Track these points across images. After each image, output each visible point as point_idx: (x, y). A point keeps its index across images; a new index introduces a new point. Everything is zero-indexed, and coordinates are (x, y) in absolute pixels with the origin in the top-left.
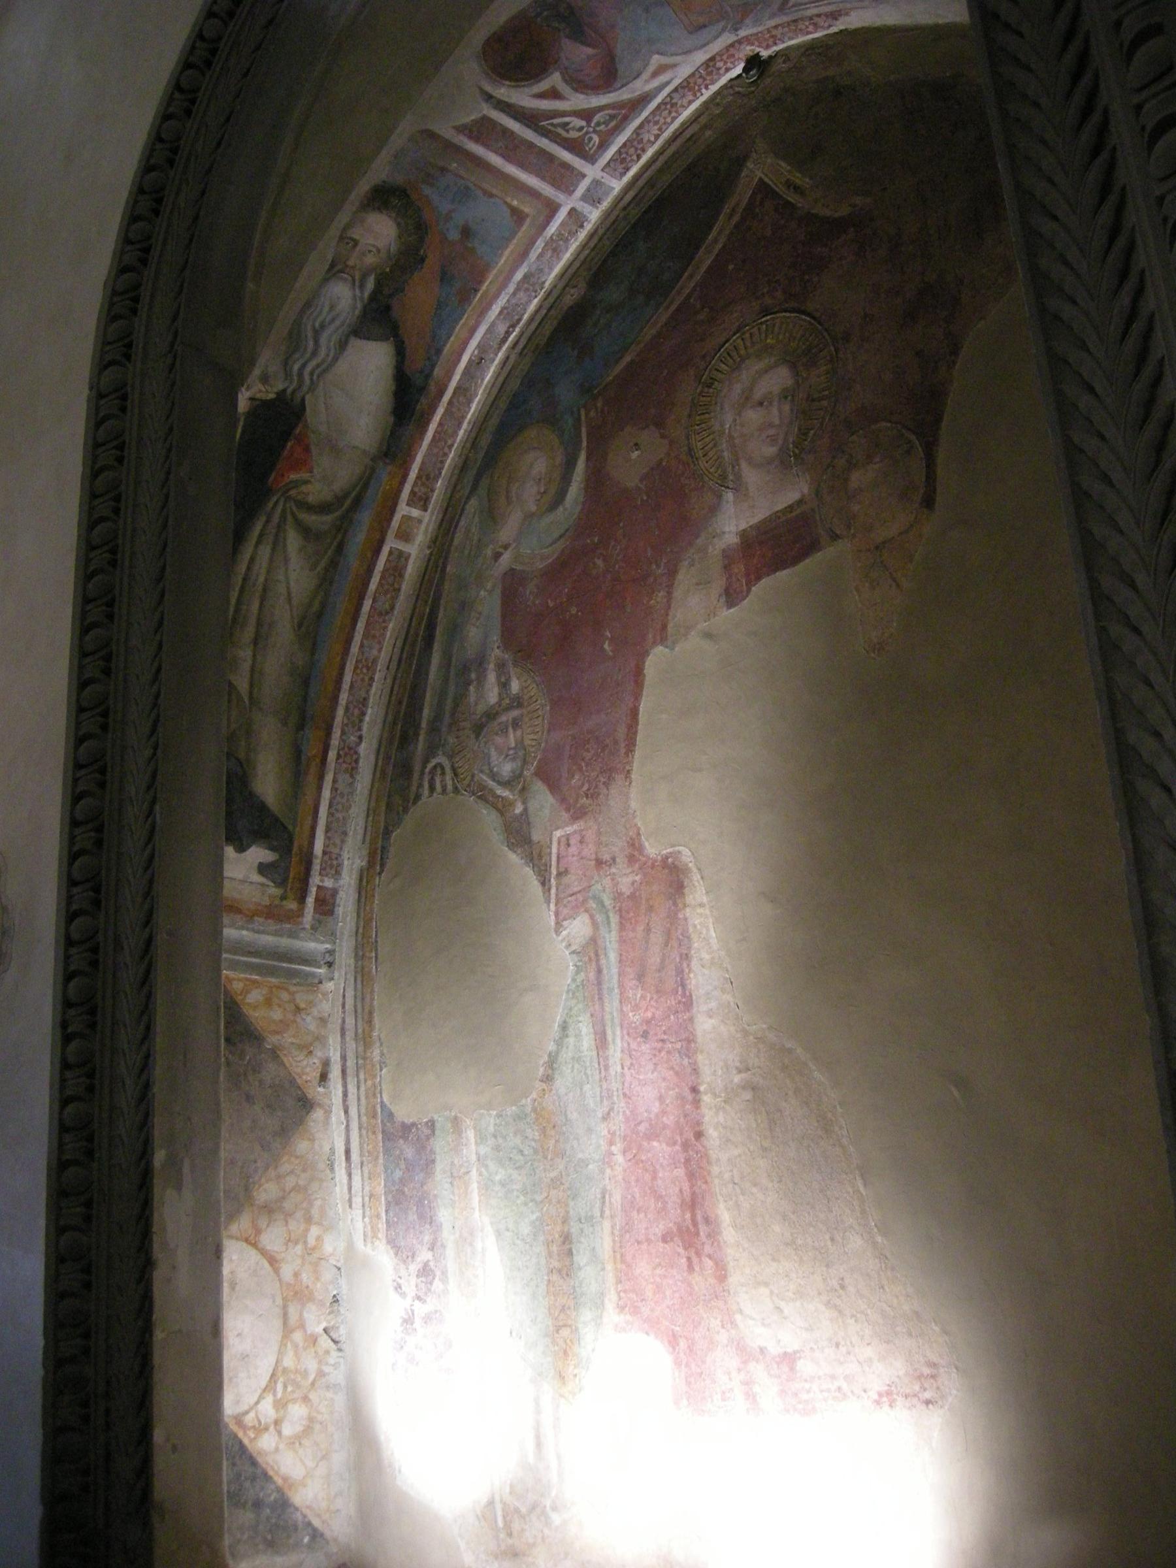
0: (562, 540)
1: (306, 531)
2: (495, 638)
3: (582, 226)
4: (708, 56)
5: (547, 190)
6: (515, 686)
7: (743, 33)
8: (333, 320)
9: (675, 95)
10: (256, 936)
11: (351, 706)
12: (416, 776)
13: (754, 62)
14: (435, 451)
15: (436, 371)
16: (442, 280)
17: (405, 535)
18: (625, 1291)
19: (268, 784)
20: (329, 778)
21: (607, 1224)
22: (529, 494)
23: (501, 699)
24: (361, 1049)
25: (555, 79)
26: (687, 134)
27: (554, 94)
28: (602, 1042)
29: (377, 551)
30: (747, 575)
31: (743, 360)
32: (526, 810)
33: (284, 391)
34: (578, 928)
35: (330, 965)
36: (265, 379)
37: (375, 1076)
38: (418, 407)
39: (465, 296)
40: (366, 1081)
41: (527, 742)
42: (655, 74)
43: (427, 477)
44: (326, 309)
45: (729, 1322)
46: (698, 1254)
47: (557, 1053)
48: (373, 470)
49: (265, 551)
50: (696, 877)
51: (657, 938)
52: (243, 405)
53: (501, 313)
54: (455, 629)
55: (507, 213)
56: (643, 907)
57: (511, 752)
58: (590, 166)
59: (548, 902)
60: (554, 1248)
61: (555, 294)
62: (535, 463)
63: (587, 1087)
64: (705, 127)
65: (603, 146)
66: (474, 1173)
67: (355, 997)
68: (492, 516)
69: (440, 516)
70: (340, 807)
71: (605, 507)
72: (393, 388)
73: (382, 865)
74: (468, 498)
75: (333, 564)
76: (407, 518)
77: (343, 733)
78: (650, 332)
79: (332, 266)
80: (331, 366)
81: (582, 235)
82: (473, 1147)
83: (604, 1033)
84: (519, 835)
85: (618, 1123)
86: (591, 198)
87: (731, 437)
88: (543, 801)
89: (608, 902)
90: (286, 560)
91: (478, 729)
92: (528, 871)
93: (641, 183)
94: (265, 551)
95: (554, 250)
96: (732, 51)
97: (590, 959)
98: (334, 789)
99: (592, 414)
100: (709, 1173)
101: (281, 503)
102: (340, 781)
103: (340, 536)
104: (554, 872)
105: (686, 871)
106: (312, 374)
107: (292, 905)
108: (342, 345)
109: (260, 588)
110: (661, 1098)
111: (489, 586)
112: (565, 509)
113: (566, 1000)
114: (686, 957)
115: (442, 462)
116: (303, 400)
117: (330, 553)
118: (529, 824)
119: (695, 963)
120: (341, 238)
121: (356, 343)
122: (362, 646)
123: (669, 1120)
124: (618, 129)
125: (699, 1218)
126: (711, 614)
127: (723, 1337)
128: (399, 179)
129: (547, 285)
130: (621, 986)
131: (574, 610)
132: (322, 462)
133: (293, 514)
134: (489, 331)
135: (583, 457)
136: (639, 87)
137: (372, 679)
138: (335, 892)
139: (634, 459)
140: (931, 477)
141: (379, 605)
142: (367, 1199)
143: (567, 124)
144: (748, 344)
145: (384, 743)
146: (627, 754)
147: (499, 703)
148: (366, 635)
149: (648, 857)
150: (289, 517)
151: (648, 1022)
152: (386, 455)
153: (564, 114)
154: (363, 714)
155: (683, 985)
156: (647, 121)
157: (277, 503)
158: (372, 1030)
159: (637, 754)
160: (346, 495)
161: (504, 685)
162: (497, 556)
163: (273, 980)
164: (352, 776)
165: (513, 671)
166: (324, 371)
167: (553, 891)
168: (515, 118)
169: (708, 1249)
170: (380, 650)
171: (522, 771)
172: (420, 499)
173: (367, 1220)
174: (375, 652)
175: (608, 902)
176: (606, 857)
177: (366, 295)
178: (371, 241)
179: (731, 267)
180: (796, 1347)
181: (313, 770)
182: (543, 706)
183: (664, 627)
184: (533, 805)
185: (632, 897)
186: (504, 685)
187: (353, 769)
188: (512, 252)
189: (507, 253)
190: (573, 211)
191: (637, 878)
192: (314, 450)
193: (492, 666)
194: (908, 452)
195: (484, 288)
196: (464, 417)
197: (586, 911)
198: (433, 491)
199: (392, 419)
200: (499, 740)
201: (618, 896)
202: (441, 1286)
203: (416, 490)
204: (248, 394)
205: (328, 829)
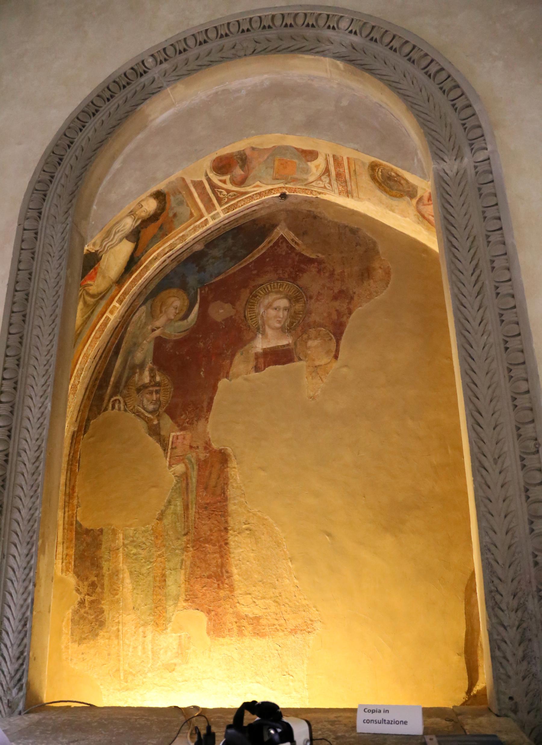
0: (185, 332)
4: (272, 188)
6: (158, 379)
7: (287, 186)
8: (122, 231)
9: (255, 196)
12: (106, 401)
13: (283, 196)
18: (189, 595)
21: (183, 572)
23: (150, 381)
24: (67, 499)
25: (227, 177)
27: (224, 182)
30: (264, 363)
31: (269, 292)
32: (159, 423)
34: (180, 468)
37: (73, 510)
38: (132, 269)
40: (68, 511)
41: (161, 399)
42: (255, 187)
43: (125, 293)
45: (233, 606)
46: (222, 583)
47: (165, 511)
48: (111, 286)
50: (233, 458)
51: (214, 476)
55: (189, 212)
56: (209, 465)
59: (166, 458)
63: (178, 524)
64: (261, 209)
65: (227, 203)
66: (121, 549)
67: (66, 479)
68: (152, 315)
69: (127, 309)
76: (115, 306)
78: (231, 272)
79: (131, 211)
80: (114, 246)
81: (205, 228)
82: (122, 541)
83: (188, 505)
87: (262, 316)
88: (167, 422)
89: (193, 461)
91: (139, 390)
92: (158, 445)
96: (280, 189)
97: (184, 480)
99: (203, 292)
100: (230, 557)
104: (170, 447)
105: (229, 455)
112: (187, 322)
113: (171, 492)
114: (227, 484)
115: (131, 289)
118: (160, 428)
119: (230, 487)
120: (139, 203)
124: (234, 199)
125: (224, 571)
126: (248, 373)
127: (231, 610)
129: (187, 241)
130: (197, 490)
134: (163, 250)
136: (248, 189)
139: (220, 312)
140: (337, 351)
142: (64, 556)
144: (272, 287)
145: (90, 386)
146: (207, 412)
147: (150, 383)
148: (90, 345)
149: (213, 449)
151: (207, 504)
153: (223, 189)
154: (81, 374)
155: (224, 494)
156: (242, 200)
158: (74, 492)
159: (212, 413)
167: (169, 454)
168: (209, 185)
169: (227, 581)
173: (64, 564)
176: (195, 445)
178: (147, 208)
179: (267, 260)
180: (260, 615)
182: (170, 388)
183: (228, 373)
184: (162, 422)
185: (205, 461)
186: (153, 377)
190: (207, 219)
191: (208, 455)
193: (147, 369)
194: (330, 340)
197: (184, 463)
200: (148, 396)
201: (198, 460)
202: (100, 590)
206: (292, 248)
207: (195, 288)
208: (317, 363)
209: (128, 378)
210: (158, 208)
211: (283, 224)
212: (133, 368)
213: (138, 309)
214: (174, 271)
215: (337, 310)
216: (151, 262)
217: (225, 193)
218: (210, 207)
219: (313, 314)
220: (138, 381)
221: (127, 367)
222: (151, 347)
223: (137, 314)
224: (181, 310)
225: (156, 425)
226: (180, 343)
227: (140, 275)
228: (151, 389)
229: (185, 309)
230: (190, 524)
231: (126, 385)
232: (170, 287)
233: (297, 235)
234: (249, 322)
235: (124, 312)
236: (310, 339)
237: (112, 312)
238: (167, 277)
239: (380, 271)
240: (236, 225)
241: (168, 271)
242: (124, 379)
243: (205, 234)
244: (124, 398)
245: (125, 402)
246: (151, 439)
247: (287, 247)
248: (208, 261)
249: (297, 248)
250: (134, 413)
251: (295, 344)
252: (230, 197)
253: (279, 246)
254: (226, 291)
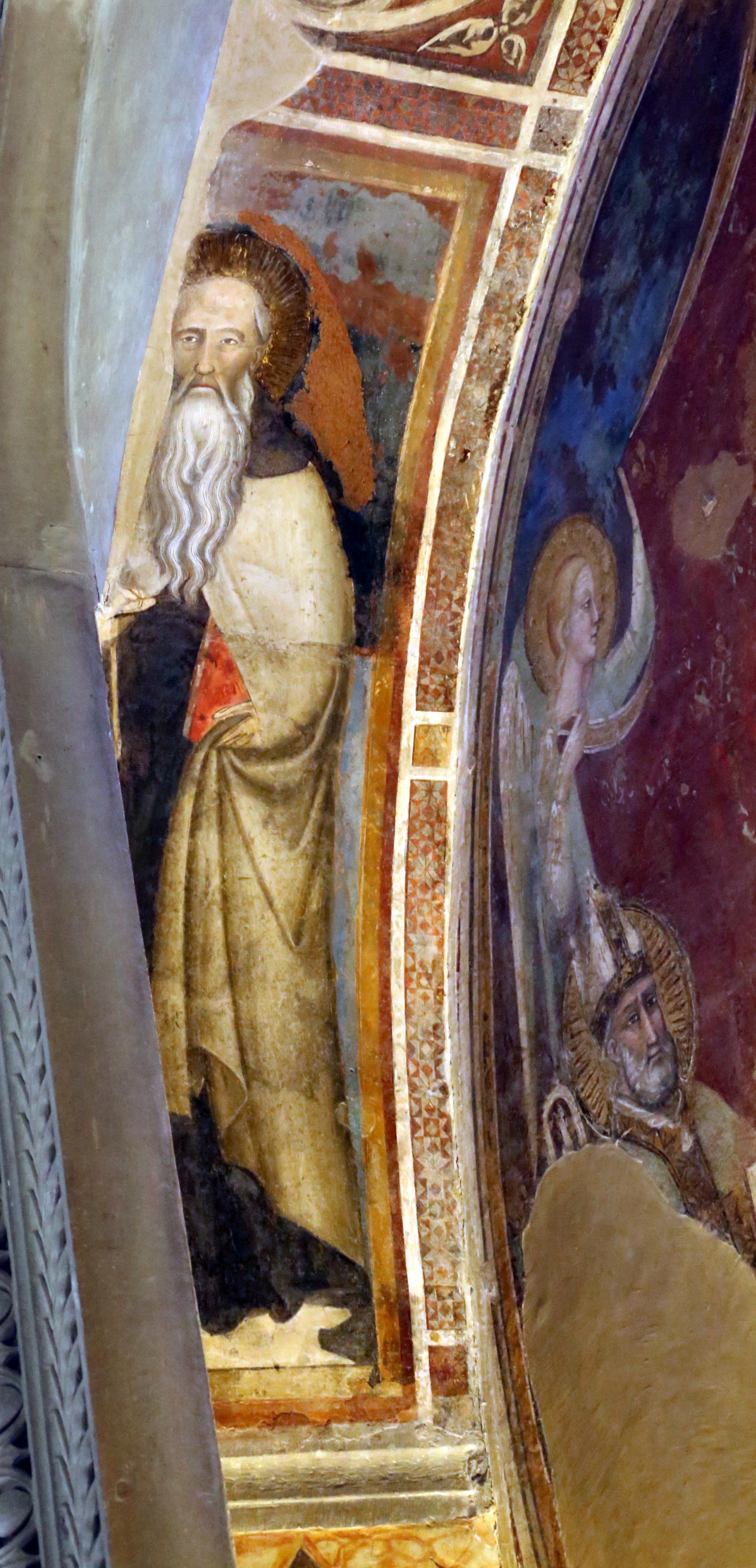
0: (643, 683)
1: (263, 791)
2: (588, 872)
3: (551, 192)
5: (471, 153)
6: (633, 941)
8: (208, 462)
10: (342, 1455)
11: (416, 1044)
12: (532, 1128)
14: (438, 613)
15: (398, 495)
16: (356, 349)
17: (428, 756)
19: (306, 1198)
20: (406, 1167)
22: (580, 629)
23: (619, 967)
29: (391, 793)
33: (166, 590)
35: (481, 1479)
36: (129, 580)
39: (405, 359)
41: (672, 1028)
43: (437, 659)
44: (191, 448)
48: (345, 671)
49: (209, 841)
52: (107, 628)
53: (470, 372)
54: (532, 877)
55: (420, 210)
57: (654, 1051)
58: (526, 89)
62: (578, 579)
65: (536, 48)
68: (540, 685)
69: (474, 711)
70: (437, 1209)
72: (339, 536)
73: (519, 1290)
75: (326, 832)
77: (413, 1088)
78: (684, 308)
79: (178, 379)
81: (557, 205)
86: (550, 139)
90: (247, 844)
91: (599, 1026)
94: (209, 841)
95: (520, 245)
98: (421, 1182)
99: (635, 471)
101: (214, 758)
102: (426, 1164)
103: (323, 785)
106: (201, 553)
107: (394, 1390)
108: (236, 497)
109: (218, 897)
111: (561, 793)
112: (634, 634)
115: (455, 629)
116: (200, 595)
117: (314, 814)
121: (252, 486)
122: (408, 944)
128: (231, 216)
129: (530, 304)
131: (685, 789)
132: (260, 680)
133: (236, 770)
134: (463, 403)
137: (440, 992)
138: (461, 1353)
141: (417, 874)
143: (463, 33)
148: (409, 929)
150: (232, 776)
152: (359, 642)
153: (451, 19)
154: (440, 1051)
157: (206, 759)
160: (314, 721)
162: (561, 741)
163: (388, 1526)
164: (445, 1154)
165: (623, 917)
166: (219, 544)
170: (441, 944)
171: (677, 1078)
172: (437, 694)
174: (433, 949)
177: (246, 407)
181: (377, 1160)
184: (706, 1131)
186: (618, 944)
187: (443, 1142)
188: (452, 271)
189: (444, 274)
190: (526, 172)
192: (241, 666)
195: (428, 340)
196: (467, 550)
198: (453, 676)
199: (351, 585)
200: (631, 1035)
203: (425, 681)
204: (110, 611)
205: (424, 1250)
207: (611, 475)
210: (268, 293)
220: (587, 986)
224: (603, 598)
225: (693, 1152)
229: (610, 585)
231: (564, 1027)
235: (473, 729)
245: (581, 1102)
250: (618, 1136)
252: (522, 19)
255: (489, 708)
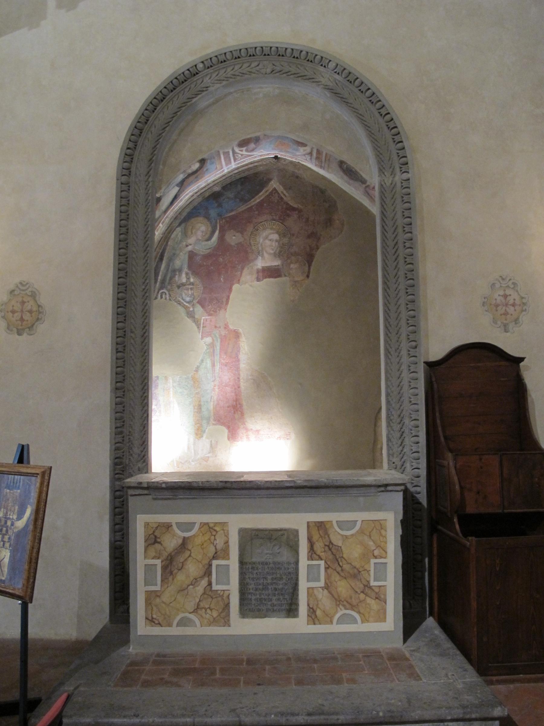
13: (276, 157)
22: (199, 234)
26: (256, 164)
28: (213, 365)
34: (209, 340)
39: (197, 181)
41: (195, 294)
50: (243, 335)
54: (170, 260)
60: (196, 407)
61: (211, 185)
62: (201, 227)
64: (261, 165)
68: (185, 234)
71: (222, 246)
74: (177, 227)
78: (240, 209)
84: (191, 315)
85: (217, 383)
87: (262, 245)
88: (199, 310)
89: (217, 336)
91: (179, 287)
92: (194, 324)
93: (240, 170)
104: (202, 326)
110: (229, 379)
114: (239, 351)
119: (241, 353)
123: (231, 383)
130: (220, 354)
135: (217, 232)
136: (254, 153)
139: (233, 238)
140: (309, 272)
161: (188, 279)
162: (187, 246)
175: (217, 336)
176: (218, 326)
183: (239, 280)
184: (195, 309)
185: (225, 336)
193: (184, 273)
200: (186, 291)
201: (220, 335)
206: (282, 198)
208: (296, 279)
209: (171, 279)
211: (275, 178)
212: (174, 271)
213: (175, 229)
214: (200, 203)
215: (310, 246)
216: (184, 197)
217: (240, 156)
218: (228, 162)
219: (294, 247)
221: (170, 270)
222: (187, 257)
223: (175, 233)
226: (207, 257)
227: (177, 205)
228: (187, 286)
229: (209, 233)
230: (216, 375)
232: (197, 216)
233: (285, 189)
234: (253, 247)
236: (292, 263)
237: (157, 231)
238: (195, 208)
239: (337, 221)
240: (243, 175)
241: (195, 203)
242: (168, 278)
243: (221, 179)
244: (169, 291)
246: (188, 319)
247: (279, 197)
248: (224, 200)
249: (285, 198)
251: (282, 265)
253: (272, 196)
254: (236, 223)
255: (171, 230)
